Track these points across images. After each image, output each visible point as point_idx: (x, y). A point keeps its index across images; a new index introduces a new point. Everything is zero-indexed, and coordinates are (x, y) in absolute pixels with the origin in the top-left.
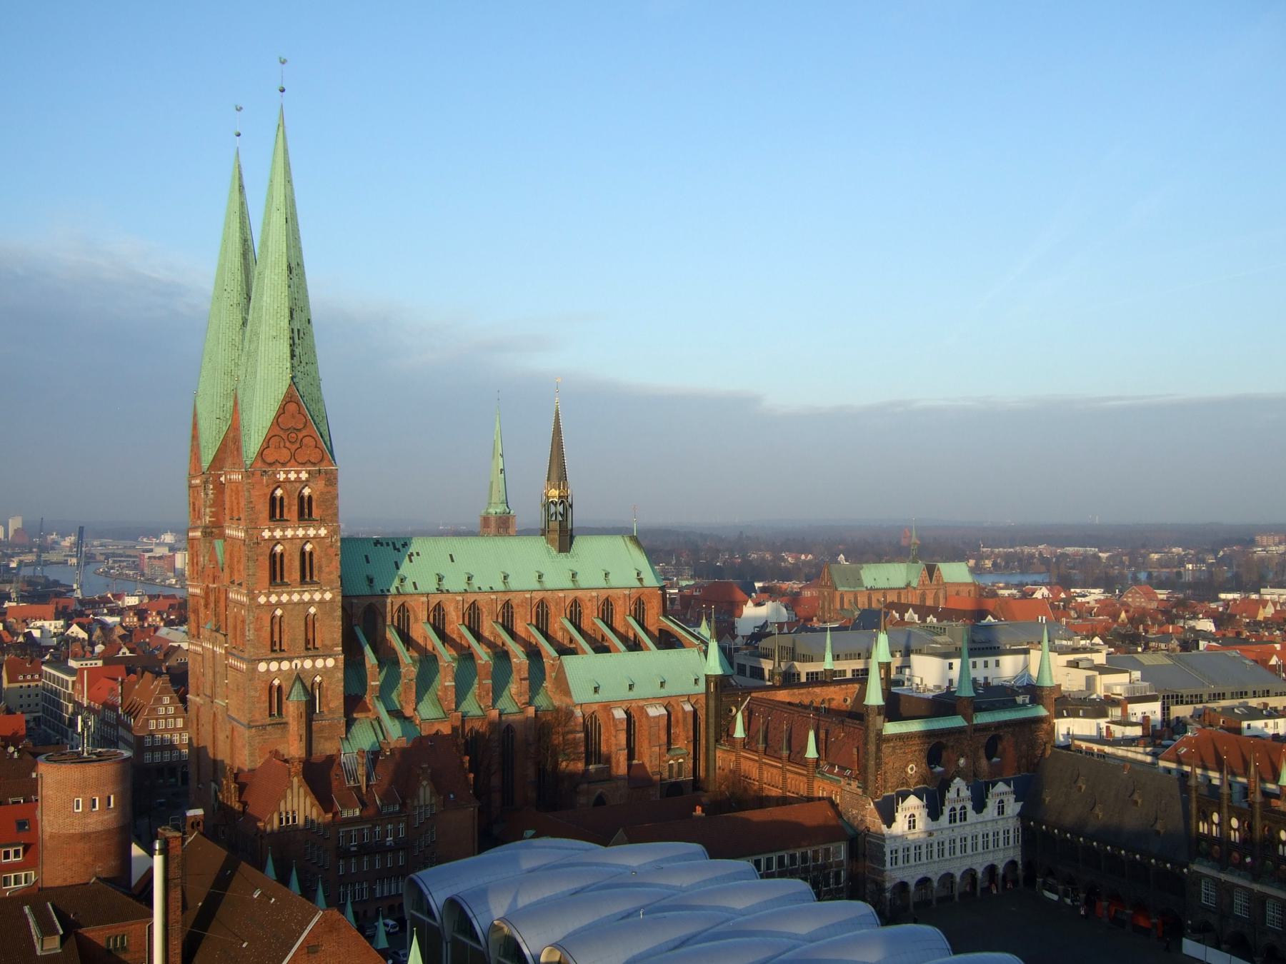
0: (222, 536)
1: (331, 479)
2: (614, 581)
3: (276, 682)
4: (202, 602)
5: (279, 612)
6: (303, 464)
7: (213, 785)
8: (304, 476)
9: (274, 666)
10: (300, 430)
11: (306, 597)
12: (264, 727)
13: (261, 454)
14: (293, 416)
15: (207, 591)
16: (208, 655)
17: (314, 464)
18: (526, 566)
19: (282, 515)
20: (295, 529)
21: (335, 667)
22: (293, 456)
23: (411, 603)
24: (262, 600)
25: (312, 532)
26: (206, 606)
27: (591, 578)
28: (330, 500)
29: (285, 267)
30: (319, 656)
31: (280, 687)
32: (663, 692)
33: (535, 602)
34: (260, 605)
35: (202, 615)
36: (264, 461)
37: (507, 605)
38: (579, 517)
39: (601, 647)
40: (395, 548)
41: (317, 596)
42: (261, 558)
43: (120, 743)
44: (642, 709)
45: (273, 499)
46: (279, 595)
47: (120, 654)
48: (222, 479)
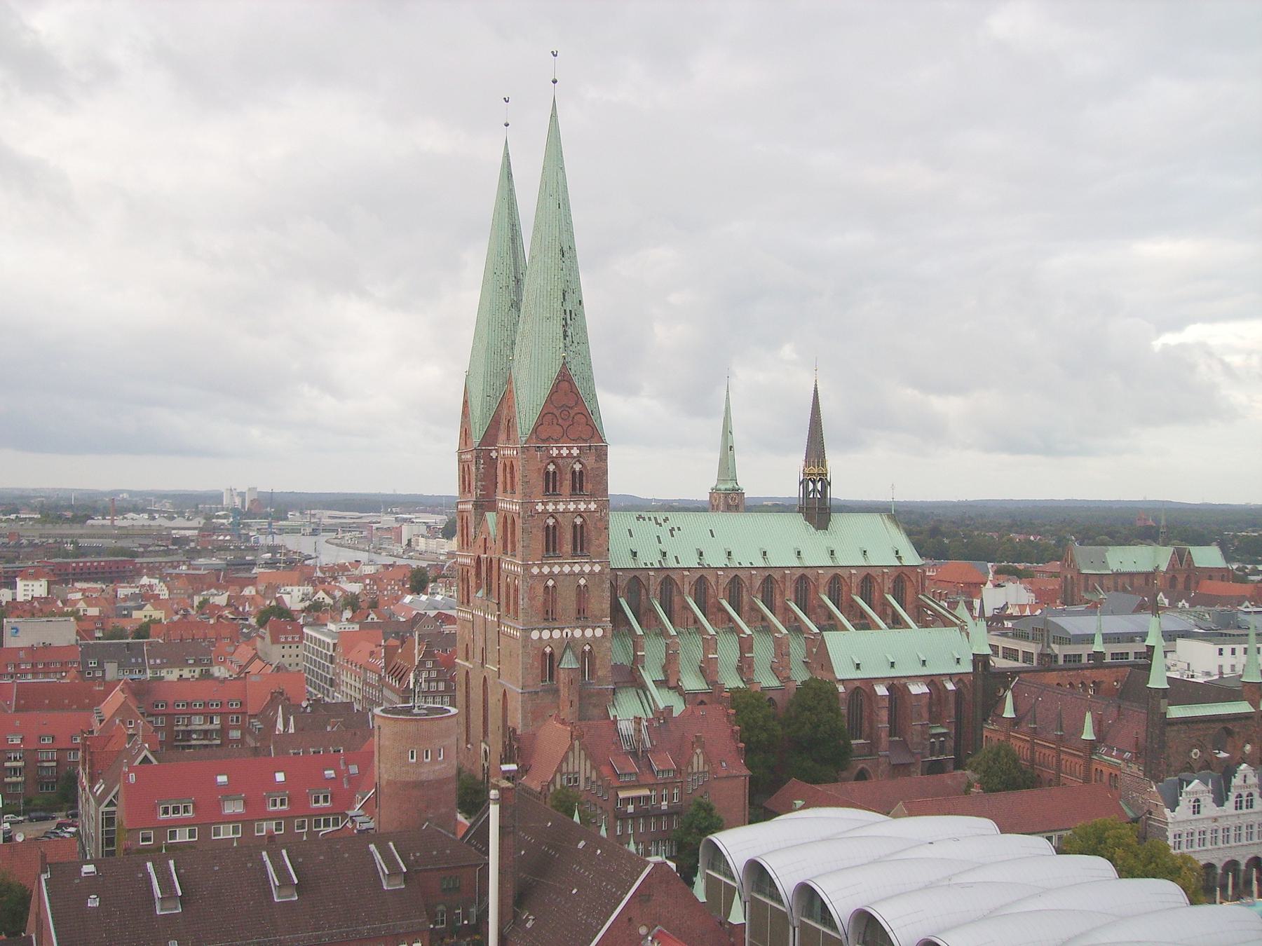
0: (492, 507)
2: (874, 561)
3: (548, 650)
4: (473, 572)
5: (551, 583)
6: (575, 440)
7: (483, 745)
8: (575, 452)
11: (577, 569)
12: (536, 693)
13: (535, 430)
16: (479, 622)
17: (585, 441)
18: (788, 545)
19: (554, 489)
22: (565, 432)
23: (674, 576)
24: (535, 570)
25: (582, 506)
26: (478, 574)
27: (849, 557)
28: (601, 475)
31: (551, 654)
33: (794, 578)
34: (533, 576)
36: (537, 437)
37: (768, 580)
38: (837, 493)
39: (863, 623)
41: (587, 569)
42: (534, 531)
44: (905, 687)
45: (548, 473)
48: (494, 454)
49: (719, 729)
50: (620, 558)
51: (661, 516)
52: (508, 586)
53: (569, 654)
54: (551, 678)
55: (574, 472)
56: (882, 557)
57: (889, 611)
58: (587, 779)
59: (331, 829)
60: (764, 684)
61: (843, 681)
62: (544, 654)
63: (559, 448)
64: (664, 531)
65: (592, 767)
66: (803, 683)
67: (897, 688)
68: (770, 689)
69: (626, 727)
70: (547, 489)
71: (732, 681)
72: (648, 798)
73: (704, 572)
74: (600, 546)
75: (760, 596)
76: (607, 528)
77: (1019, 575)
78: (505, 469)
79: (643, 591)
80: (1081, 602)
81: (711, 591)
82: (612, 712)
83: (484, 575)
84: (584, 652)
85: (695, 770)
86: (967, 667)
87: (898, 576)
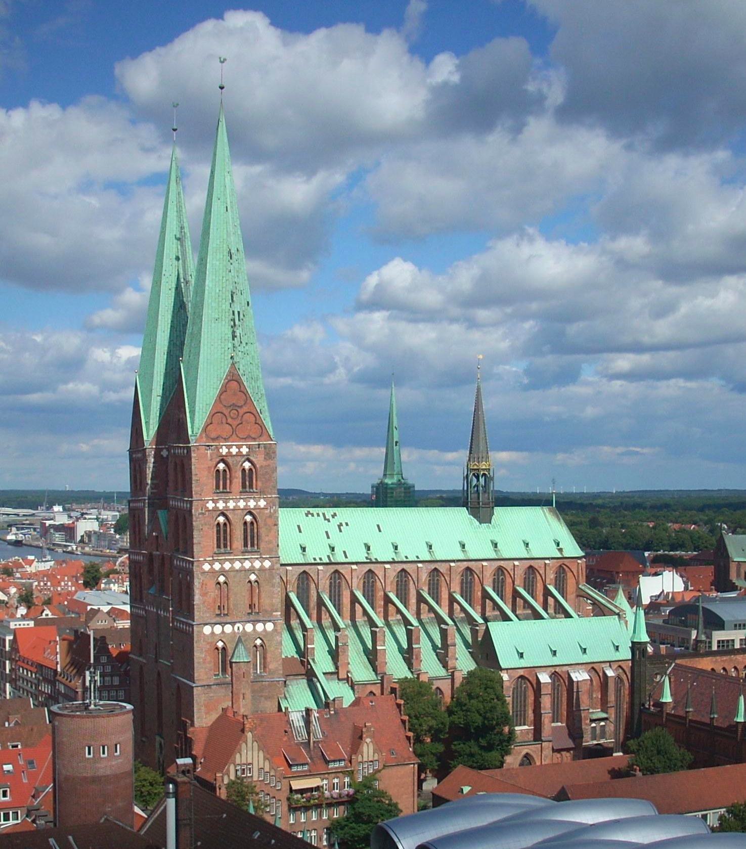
0: (165, 506)
1: (270, 453)
3: (220, 644)
4: (145, 569)
5: (222, 579)
6: (245, 439)
7: (158, 738)
8: (244, 450)
9: (218, 629)
10: (241, 407)
11: (247, 565)
13: (205, 429)
14: (235, 394)
15: (151, 557)
17: (254, 439)
19: (225, 487)
20: (237, 500)
21: (275, 630)
22: (234, 431)
23: (342, 569)
24: (206, 567)
25: (252, 504)
26: (151, 571)
27: (511, 549)
29: (226, 253)
30: (259, 621)
31: (224, 649)
32: (586, 659)
34: (204, 572)
35: (145, 581)
40: (325, 519)
41: (257, 564)
42: (206, 528)
43: (61, 699)
46: (222, 562)
47: (44, 616)
49: (389, 719)
50: (289, 552)
51: (329, 512)
52: (180, 583)
53: (241, 648)
54: (224, 670)
55: (244, 470)
56: (543, 548)
57: (551, 600)
58: (260, 769)
59: (11, 822)
60: (432, 674)
61: (507, 669)
62: (217, 648)
63: (229, 447)
64: (332, 527)
65: (265, 758)
66: (471, 674)
67: (560, 677)
68: (437, 679)
69: (297, 718)
70: (218, 487)
71: (397, 669)
72: (318, 788)
73: (372, 567)
74: (270, 542)
75: (426, 589)
76: (276, 525)
77: (674, 563)
78: (175, 469)
79: (313, 586)
80: (734, 588)
81: (378, 584)
82: (284, 705)
83: (156, 571)
84: (255, 646)
85: (365, 759)
86: (625, 654)
87: (560, 566)
